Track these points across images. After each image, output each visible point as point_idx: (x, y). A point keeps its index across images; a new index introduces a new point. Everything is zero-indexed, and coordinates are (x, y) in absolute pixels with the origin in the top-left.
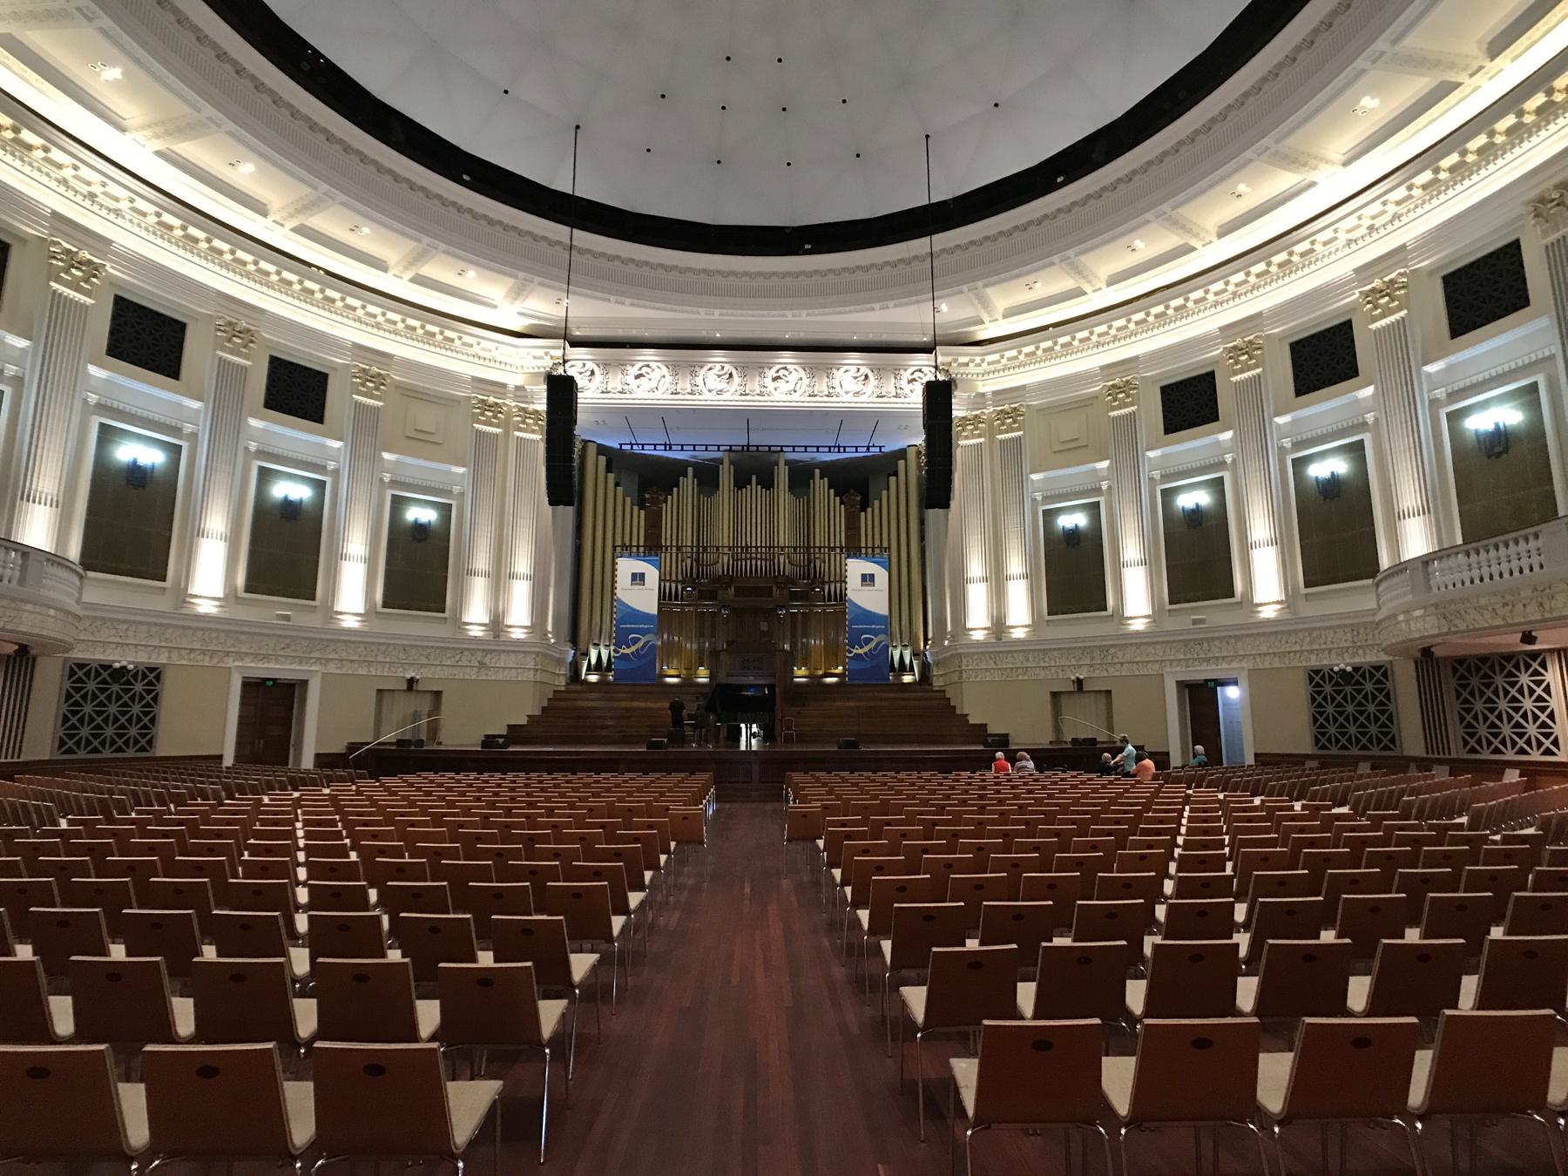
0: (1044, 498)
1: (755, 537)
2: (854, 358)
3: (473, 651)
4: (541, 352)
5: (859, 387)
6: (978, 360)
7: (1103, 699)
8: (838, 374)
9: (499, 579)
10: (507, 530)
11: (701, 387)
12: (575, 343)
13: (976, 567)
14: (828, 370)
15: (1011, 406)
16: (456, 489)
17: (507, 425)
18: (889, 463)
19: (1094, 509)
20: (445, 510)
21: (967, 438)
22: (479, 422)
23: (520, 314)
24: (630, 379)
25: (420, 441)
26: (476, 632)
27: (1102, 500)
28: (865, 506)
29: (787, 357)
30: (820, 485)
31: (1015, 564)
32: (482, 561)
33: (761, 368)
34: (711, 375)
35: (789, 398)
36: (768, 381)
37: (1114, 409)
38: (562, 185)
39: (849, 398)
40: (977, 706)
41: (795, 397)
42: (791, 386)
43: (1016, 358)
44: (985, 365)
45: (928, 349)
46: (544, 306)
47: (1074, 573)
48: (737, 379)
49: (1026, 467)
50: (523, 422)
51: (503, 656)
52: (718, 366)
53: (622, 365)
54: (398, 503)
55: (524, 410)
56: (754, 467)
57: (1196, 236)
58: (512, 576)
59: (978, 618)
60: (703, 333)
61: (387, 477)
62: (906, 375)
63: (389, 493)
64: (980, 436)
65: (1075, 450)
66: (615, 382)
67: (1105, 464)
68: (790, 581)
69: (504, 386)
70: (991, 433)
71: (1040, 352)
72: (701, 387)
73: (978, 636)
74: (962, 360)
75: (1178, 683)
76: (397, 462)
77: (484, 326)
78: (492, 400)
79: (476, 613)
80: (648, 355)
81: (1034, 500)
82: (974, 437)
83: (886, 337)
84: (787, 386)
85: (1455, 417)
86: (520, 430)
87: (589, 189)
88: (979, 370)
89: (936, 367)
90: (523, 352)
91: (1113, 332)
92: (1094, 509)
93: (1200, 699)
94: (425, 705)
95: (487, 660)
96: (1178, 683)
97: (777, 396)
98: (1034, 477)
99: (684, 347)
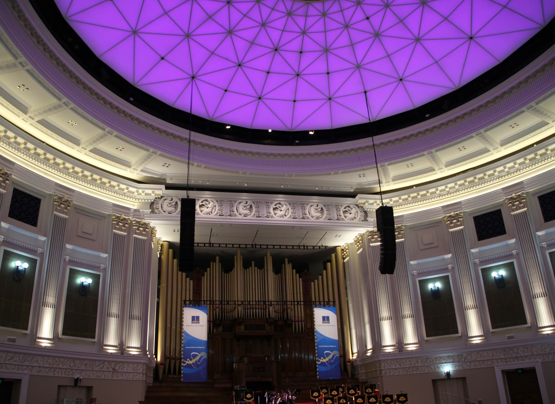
0: (418, 274)
3: (110, 362)
4: (150, 192)
8: (308, 207)
10: (128, 291)
14: (303, 205)
16: (102, 266)
17: (129, 230)
22: (116, 229)
26: (111, 350)
27: (449, 274)
29: (280, 198)
31: (407, 311)
32: (115, 309)
33: (267, 204)
35: (282, 219)
36: (271, 210)
39: (312, 220)
41: (286, 218)
42: (282, 213)
43: (398, 201)
45: (353, 195)
47: (439, 315)
48: (254, 209)
50: (138, 229)
51: (126, 365)
57: (492, 145)
58: (131, 317)
60: (237, 184)
67: (450, 256)
69: (129, 209)
71: (410, 199)
74: (371, 201)
77: (119, 177)
78: (123, 216)
81: (413, 275)
83: (332, 189)
86: (136, 233)
90: (140, 191)
91: (447, 189)
92: (445, 280)
95: (117, 368)
97: (276, 218)
98: (412, 263)
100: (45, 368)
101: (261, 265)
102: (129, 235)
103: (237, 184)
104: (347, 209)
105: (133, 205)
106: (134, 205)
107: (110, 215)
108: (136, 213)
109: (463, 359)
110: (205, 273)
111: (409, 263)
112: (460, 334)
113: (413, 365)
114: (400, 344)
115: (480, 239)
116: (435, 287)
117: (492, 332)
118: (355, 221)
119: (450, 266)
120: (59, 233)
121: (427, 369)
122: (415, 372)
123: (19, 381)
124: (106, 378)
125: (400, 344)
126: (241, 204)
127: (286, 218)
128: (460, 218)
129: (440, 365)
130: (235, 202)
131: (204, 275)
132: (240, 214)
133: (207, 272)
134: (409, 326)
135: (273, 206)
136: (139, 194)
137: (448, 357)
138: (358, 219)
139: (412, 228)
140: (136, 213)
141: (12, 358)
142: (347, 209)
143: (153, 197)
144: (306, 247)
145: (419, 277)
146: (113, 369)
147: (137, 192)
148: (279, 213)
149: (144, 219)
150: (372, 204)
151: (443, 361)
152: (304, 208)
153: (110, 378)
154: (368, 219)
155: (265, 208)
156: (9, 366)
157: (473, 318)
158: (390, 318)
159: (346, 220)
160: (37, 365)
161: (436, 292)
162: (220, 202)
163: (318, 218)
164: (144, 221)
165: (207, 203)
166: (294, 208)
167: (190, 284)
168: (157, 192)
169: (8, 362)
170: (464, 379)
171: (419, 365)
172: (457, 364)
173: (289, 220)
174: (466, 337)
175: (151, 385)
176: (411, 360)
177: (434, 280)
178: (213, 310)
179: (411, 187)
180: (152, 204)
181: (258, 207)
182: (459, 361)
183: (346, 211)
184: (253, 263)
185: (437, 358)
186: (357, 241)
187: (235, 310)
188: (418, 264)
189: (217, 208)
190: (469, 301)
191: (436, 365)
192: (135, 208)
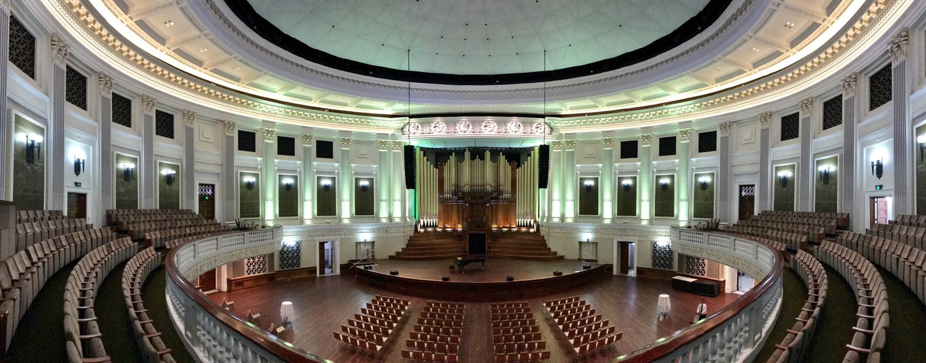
1: (478, 181)
2: (515, 119)
8: (509, 125)
9: (390, 201)
12: (411, 117)
13: (556, 195)
14: (505, 123)
15: (571, 140)
18: (528, 151)
19: (596, 180)
20: (371, 180)
24: (432, 128)
25: (362, 157)
28: (519, 166)
30: (502, 158)
32: (384, 196)
38: (404, 67)
40: (554, 245)
46: (400, 107)
47: (588, 201)
53: (429, 123)
56: (477, 153)
59: (556, 214)
65: (592, 158)
66: (427, 130)
68: (491, 193)
73: (556, 220)
75: (619, 242)
79: (383, 213)
80: (438, 119)
85: (697, 176)
87: (416, 66)
93: (624, 247)
94: (369, 247)
96: (619, 242)
97: (486, 133)
102: (389, 151)
105: (390, 132)
114: (563, 218)
125: (563, 218)
135: (484, 124)
143: (402, 125)
148: (488, 129)
152: (506, 125)
159: (537, 134)
162: (447, 123)
166: (499, 125)
167: (436, 171)
174: (601, 218)
177: (590, 179)
180: (402, 129)
181: (473, 126)
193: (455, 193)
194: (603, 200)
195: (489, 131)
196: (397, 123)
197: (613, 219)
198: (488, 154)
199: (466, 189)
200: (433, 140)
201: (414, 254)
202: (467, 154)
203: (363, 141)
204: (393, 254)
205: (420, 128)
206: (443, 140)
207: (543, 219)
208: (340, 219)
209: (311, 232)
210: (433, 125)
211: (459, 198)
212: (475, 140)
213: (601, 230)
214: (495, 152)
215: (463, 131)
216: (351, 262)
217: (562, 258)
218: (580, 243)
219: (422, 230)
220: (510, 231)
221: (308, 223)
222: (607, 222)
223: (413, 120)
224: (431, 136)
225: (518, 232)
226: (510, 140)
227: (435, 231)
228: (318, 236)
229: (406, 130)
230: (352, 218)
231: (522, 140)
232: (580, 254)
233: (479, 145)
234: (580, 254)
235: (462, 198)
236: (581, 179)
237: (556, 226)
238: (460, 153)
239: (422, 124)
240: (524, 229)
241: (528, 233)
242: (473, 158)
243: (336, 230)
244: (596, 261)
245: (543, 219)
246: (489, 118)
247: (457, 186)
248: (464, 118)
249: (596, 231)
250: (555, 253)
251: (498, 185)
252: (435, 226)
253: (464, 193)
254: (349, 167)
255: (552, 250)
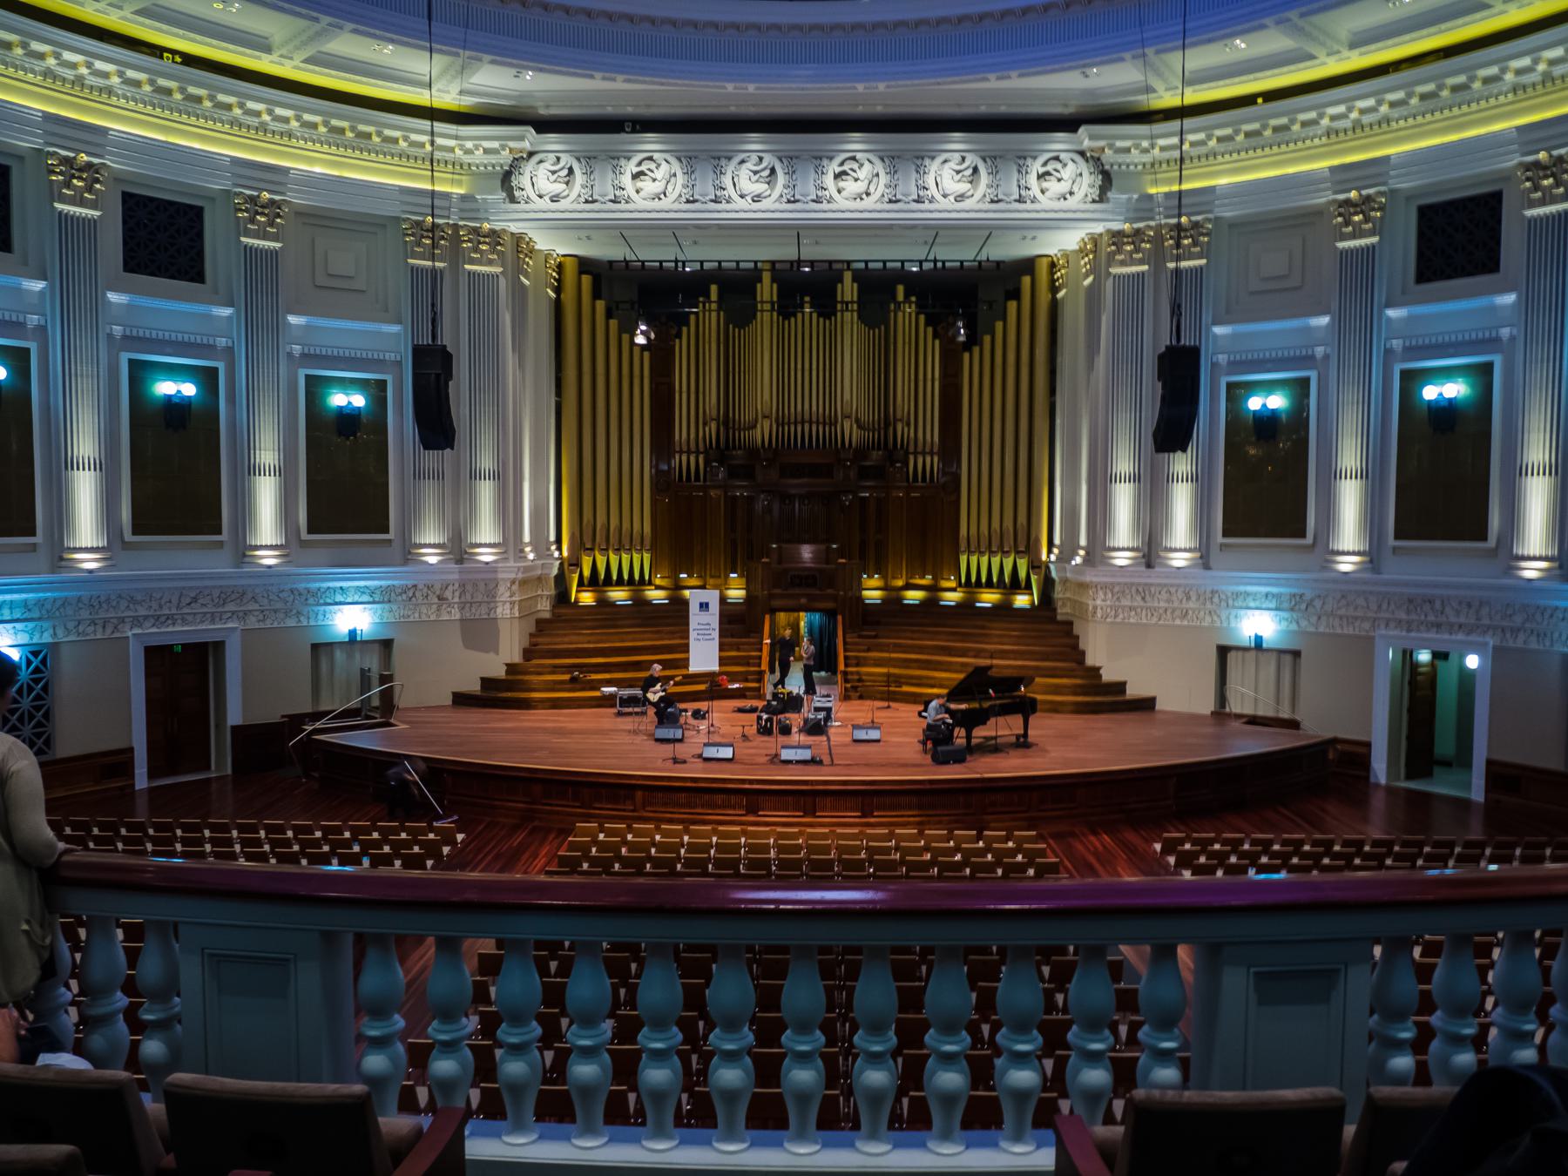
0: (1230, 363)
1: (811, 404)
5: (964, 187)
6: (1145, 144)
7: (1288, 658)
8: (933, 167)
11: (730, 191)
12: (545, 125)
14: (919, 159)
21: (1123, 263)
23: (461, 92)
30: (906, 315)
34: (744, 173)
35: (858, 205)
37: (1344, 237)
39: (949, 203)
42: (860, 187)
44: (1156, 151)
45: (1068, 124)
46: (494, 81)
49: (1207, 317)
50: (476, 250)
52: (754, 157)
54: (315, 387)
55: (476, 231)
61: (297, 349)
62: (1036, 167)
63: (302, 373)
64: (1141, 262)
66: (604, 188)
70: (1157, 257)
72: (730, 191)
73: (1122, 559)
76: (307, 327)
81: (1214, 365)
82: (1133, 262)
84: (854, 190)
86: (472, 261)
88: (1147, 158)
89: (1082, 153)
90: (469, 145)
92: (1300, 388)
94: (373, 663)
95: (448, 594)
97: (841, 202)
98: (1218, 330)
99: (703, 130)
100: (275, 611)
101: (827, 307)
102: (455, 264)
103: (733, 109)
104: (1049, 168)
106: (460, 183)
107: (397, 218)
108: (467, 205)
109: (1303, 606)
110: (685, 329)
111: (1208, 330)
112: (1309, 540)
113: (1176, 604)
115: (1423, 276)
116: (1264, 405)
117: (1395, 549)
118: (1072, 202)
119: (1320, 351)
120: (262, 286)
121: (1208, 619)
122: (1178, 622)
123: (219, 646)
124: (424, 618)
126: (744, 166)
127: (868, 203)
128: (1374, 209)
129: (1242, 612)
130: (729, 159)
131: (679, 335)
132: (742, 196)
133: (688, 325)
134: (1182, 501)
135: (834, 167)
136: (468, 152)
137: (1267, 595)
138: (1079, 195)
139: (1234, 225)
140: (467, 205)
141: (195, 600)
142: (1049, 168)
143: (505, 157)
144: (939, 265)
145: (1229, 374)
146: (440, 598)
147: (462, 147)
149: (488, 220)
150: (1128, 150)
151: (1252, 604)
152: (920, 170)
153: (433, 618)
154: (1110, 195)
155: (813, 175)
156: (190, 618)
157: (1350, 500)
158: (1136, 478)
159: (1045, 202)
160: (256, 607)
161: (1267, 424)
163: (960, 198)
164: (486, 226)
165: (653, 166)
166: (892, 172)
168: (512, 144)
169: (186, 610)
170: (1296, 654)
171: (1191, 605)
172: (1285, 615)
173: (879, 206)
175: (547, 615)
176: (1173, 590)
177: (1269, 387)
178: (705, 424)
179: (1248, 100)
182: (1292, 609)
183: (1048, 173)
184: (807, 299)
185: (1237, 595)
186: (1082, 252)
187: (755, 427)
188: (1234, 336)
189: (681, 179)
190: (1350, 456)
191: (1234, 612)
192: (462, 191)
193: (719, 453)
194: (1330, 476)
195: (854, 190)
196: (482, 147)
197: (1373, 556)
198: (848, 290)
199: (763, 432)
200: (624, 231)
201: (556, 686)
202: (767, 290)
203: (336, 220)
204: (475, 687)
205: (579, 178)
206: (673, 230)
207: (1065, 558)
208: (243, 550)
209: (94, 602)
210: (631, 167)
211: (733, 473)
212: (798, 232)
213: (1320, 600)
214: (879, 287)
215: (752, 193)
216: (296, 721)
217: (1146, 705)
218: (1223, 651)
219: (587, 598)
220: (931, 605)
221: (90, 563)
222: (1346, 565)
223: (553, 142)
224: (621, 212)
225: (967, 609)
226: (937, 231)
227: (640, 603)
228: (137, 621)
229: (523, 180)
230: (290, 546)
231: (988, 231)
232: (1222, 699)
233: (809, 253)
234: (1222, 699)
235: (746, 472)
236: (1231, 387)
237: (1122, 586)
238: (736, 287)
239: (589, 159)
240: (988, 598)
241: (1004, 610)
242: (786, 307)
243: (226, 595)
244: (1293, 725)
245: (1065, 558)
246: (855, 143)
247: (726, 422)
248: (754, 143)
249: (1293, 605)
250: (1120, 687)
251: (888, 422)
252: (636, 584)
253: (753, 452)
254: (277, 327)
255: (1107, 676)
